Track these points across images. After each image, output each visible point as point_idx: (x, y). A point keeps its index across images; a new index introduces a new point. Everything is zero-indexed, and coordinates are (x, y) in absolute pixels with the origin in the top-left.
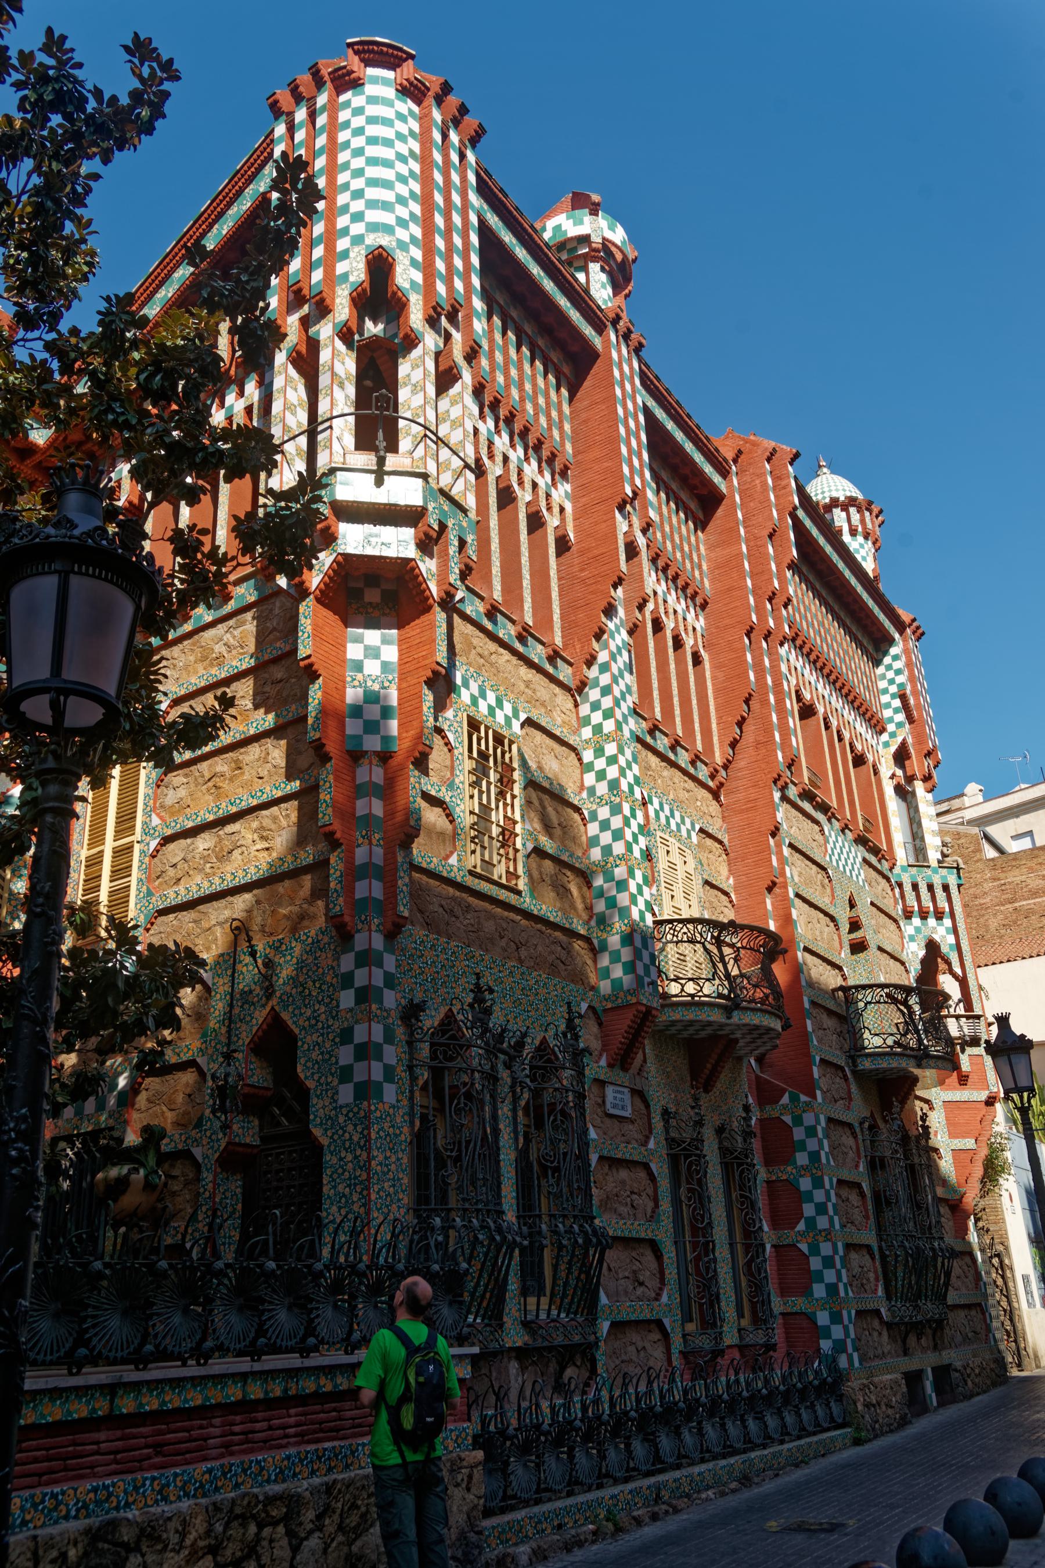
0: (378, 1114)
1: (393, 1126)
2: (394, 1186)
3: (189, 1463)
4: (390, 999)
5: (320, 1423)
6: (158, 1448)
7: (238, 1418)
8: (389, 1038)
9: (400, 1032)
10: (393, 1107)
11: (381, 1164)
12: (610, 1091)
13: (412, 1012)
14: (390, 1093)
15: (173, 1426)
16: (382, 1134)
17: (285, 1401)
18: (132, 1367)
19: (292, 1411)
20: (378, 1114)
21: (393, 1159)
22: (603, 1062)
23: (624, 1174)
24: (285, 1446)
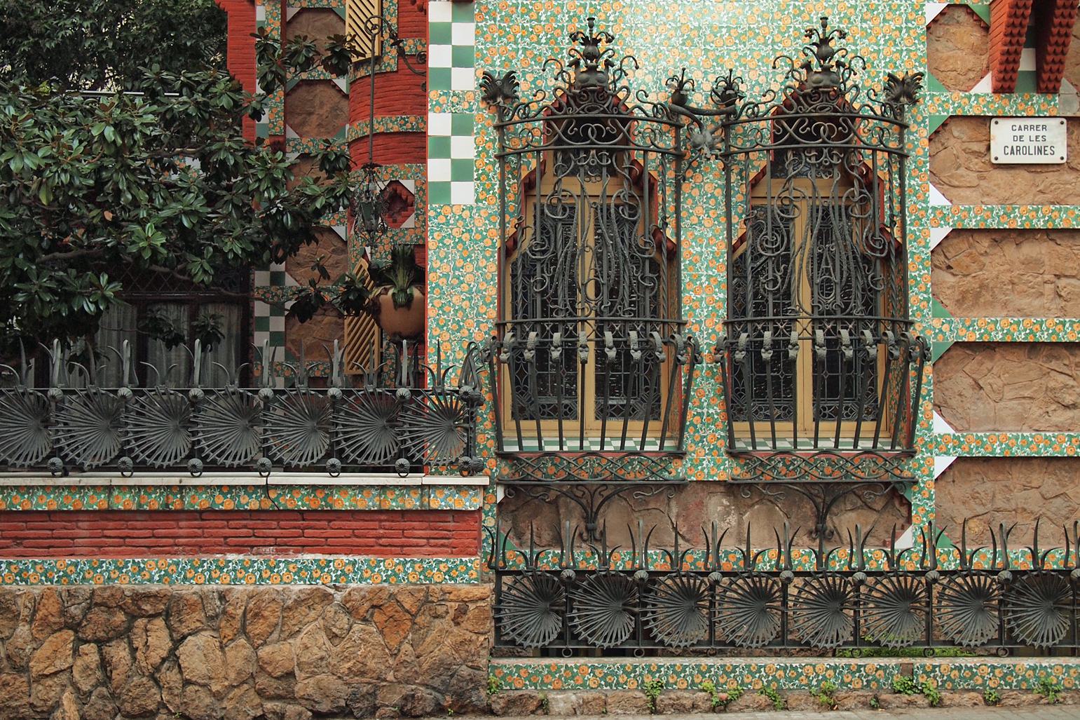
0: (442, 219)
1: (469, 231)
2: (470, 299)
3: (53, 556)
4: (466, 81)
5: (226, 538)
6: (18, 540)
7: (111, 524)
8: (461, 127)
9: (485, 117)
10: (471, 208)
11: (447, 276)
12: (1002, 134)
13: (498, 91)
14: (463, 193)
15: (31, 524)
16: (447, 241)
17: (165, 514)
18: (189, 474)
19: (182, 524)
20: (442, 219)
21: (470, 268)
22: (985, 86)
23: (1030, 249)
24: (175, 553)
